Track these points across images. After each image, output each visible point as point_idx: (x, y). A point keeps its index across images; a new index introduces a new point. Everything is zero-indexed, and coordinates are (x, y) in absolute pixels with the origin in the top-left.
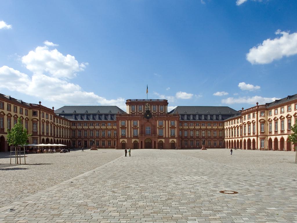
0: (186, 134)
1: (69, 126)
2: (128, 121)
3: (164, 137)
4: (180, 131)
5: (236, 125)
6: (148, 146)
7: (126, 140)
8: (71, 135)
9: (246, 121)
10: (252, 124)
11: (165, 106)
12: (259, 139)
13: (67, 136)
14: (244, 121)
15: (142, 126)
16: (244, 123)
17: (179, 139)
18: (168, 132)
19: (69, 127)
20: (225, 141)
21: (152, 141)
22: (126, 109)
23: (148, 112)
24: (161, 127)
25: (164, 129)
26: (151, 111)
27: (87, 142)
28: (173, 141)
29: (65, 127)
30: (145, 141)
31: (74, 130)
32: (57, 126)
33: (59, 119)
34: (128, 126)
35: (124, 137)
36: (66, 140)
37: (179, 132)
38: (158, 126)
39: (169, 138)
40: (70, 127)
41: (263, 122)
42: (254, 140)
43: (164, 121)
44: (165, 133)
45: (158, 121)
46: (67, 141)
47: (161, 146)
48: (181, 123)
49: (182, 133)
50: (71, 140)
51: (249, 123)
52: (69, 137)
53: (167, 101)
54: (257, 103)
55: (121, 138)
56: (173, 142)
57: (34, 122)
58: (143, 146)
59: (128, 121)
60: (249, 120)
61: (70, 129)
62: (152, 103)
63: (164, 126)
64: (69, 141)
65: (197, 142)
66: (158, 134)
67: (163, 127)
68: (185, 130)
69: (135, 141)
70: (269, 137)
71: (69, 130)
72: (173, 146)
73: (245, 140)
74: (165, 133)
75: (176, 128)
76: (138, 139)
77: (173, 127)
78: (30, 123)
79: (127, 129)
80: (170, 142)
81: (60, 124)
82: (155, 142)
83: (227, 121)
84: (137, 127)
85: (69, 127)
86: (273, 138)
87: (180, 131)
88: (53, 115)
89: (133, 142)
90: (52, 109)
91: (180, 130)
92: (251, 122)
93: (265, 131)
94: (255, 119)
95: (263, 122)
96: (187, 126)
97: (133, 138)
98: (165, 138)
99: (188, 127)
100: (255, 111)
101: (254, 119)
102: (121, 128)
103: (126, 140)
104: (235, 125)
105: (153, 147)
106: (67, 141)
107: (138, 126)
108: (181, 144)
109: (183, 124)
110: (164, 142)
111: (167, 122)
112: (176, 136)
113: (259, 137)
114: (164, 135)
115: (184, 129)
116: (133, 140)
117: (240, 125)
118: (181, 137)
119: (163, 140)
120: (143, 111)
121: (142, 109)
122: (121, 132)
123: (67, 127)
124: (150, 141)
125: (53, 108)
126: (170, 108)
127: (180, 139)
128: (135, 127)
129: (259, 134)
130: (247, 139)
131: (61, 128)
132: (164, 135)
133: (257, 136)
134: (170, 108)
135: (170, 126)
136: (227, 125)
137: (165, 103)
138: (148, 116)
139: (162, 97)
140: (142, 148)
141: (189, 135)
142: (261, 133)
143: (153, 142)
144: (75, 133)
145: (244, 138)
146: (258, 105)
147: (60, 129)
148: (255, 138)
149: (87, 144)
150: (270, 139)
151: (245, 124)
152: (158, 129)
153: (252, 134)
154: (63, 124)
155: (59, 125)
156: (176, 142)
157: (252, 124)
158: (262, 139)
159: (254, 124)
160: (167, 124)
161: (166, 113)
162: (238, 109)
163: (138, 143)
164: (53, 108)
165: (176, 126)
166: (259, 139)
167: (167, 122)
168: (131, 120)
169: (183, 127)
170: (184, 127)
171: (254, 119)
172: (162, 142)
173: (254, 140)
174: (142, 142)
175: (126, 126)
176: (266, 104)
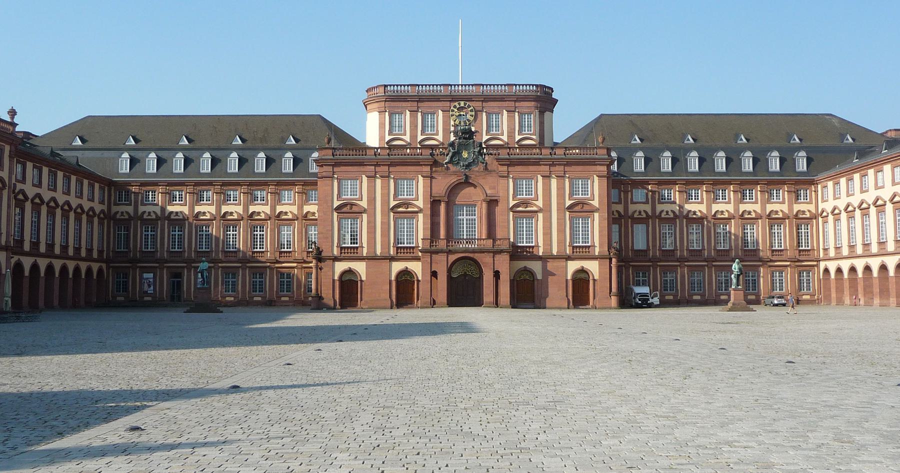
0: (640, 239)
1: (102, 202)
2: (372, 177)
5: (870, 198)
7: (360, 268)
8: (108, 243)
11: (542, 113)
13: (90, 251)
17: (611, 259)
18: (561, 231)
19: (98, 208)
20: (826, 271)
24: (524, 211)
27: (179, 275)
28: (583, 271)
29: (80, 206)
30: (449, 271)
31: (125, 223)
32: (38, 202)
33: (45, 170)
34: (372, 200)
36: (71, 265)
40: (105, 207)
46: (89, 270)
47: (526, 293)
49: (625, 236)
50: (108, 268)
52: (100, 252)
55: (336, 259)
56: (583, 276)
58: (442, 294)
59: (372, 177)
61: (107, 217)
63: (540, 203)
64: (100, 271)
67: (535, 205)
68: (639, 221)
69: (405, 272)
71: (101, 223)
75: (593, 211)
76: (417, 259)
77: (579, 209)
81: (55, 190)
82: (497, 275)
83: (835, 178)
85: (98, 208)
87: (615, 228)
88: (7, 148)
90: (9, 120)
96: (647, 202)
99: (648, 208)
102: (338, 208)
104: (879, 193)
106: (89, 270)
107: (420, 203)
109: (626, 192)
110: (539, 277)
111: (554, 182)
112: (597, 251)
115: (632, 217)
119: (536, 267)
123: (92, 209)
124: (471, 270)
125: (13, 113)
126: (565, 124)
131: (84, 217)
132: (541, 243)
134: (565, 124)
136: (834, 195)
137: (544, 100)
138: (465, 155)
141: (654, 246)
144: (127, 237)
147: (78, 219)
149: (179, 285)
154: (68, 193)
155: (47, 195)
163: (418, 281)
164: (13, 113)
165: (596, 203)
167: (554, 182)
169: (626, 208)
170: (632, 208)
172: (531, 273)
174: (434, 274)
175: (364, 204)
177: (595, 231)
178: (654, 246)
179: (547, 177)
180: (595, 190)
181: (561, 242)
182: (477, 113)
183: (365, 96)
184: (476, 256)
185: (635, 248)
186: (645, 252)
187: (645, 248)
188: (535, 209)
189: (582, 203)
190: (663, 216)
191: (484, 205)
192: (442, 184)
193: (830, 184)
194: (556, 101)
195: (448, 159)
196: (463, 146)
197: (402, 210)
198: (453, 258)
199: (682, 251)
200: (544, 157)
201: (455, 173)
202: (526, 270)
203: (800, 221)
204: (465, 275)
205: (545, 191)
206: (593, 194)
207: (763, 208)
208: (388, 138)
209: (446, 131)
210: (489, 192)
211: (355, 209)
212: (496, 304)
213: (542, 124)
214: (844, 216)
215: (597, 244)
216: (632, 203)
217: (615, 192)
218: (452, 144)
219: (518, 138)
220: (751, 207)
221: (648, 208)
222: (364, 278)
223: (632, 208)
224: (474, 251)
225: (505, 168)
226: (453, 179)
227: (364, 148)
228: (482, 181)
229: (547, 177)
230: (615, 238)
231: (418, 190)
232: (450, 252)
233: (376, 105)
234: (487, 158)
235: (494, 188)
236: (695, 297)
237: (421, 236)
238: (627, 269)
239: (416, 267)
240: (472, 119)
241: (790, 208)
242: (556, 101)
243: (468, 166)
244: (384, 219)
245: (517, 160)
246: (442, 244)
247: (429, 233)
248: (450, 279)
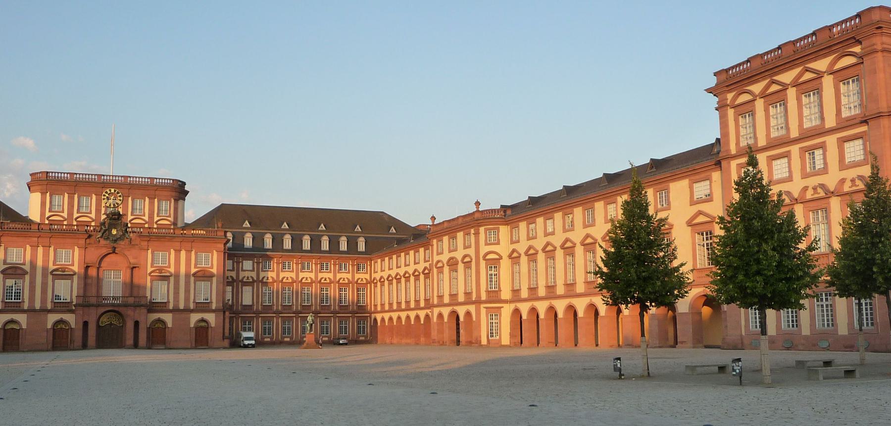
0: (247, 297)
3: (171, 307)
4: (229, 289)
7: (22, 318)
9: (445, 257)
10: (461, 267)
11: (176, 200)
12: (483, 312)
14: (436, 258)
16: (438, 262)
17: (224, 312)
18: (187, 291)
20: (375, 319)
21: (124, 322)
23: (115, 218)
25: (172, 279)
26: (126, 215)
37: (224, 292)
38: (150, 270)
39: (187, 310)
42: (468, 314)
43: (172, 252)
44: (176, 293)
45: (150, 251)
47: (158, 338)
49: (236, 294)
51: (453, 264)
53: (184, 184)
54: (478, 204)
56: (203, 324)
60: (452, 255)
62: (129, 187)
65: (284, 323)
66: (148, 295)
69: (61, 321)
70: (512, 306)
72: (201, 338)
73: (440, 316)
74: (176, 293)
76: (72, 311)
79: (27, 277)
80: (192, 325)
82: (137, 324)
84: (72, 270)
86: (525, 308)
87: (229, 289)
89: (49, 326)
91: (229, 284)
92: (460, 259)
93: (500, 288)
94: (471, 252)
96: (253, 270)
97: (50, 311)
98: (176, 310)
99: (254, 274)
100: (472, 227)
101: (468, 251)
103: (22, 318)
105: (130, 341)
108: (231, 329)
109: (238, 263)
110: (170, 325)
111: (183, 254)
113: (482, 306)
114: (171, 300)
115: (242, 281)
116: (52, 318)
117: (425, 268)
118: (232, 306)
119: (168, 318)
120: (93, 215)
126: (194, 209)
127: (227, 313)
129: (484, 297)
130: (446, 311)
132: (171, 300)
135: (193, 270)
136: (384, 268)
137: (179, 191)
138: (114, 232)
139: (165, 172)
140: (85, 346)
141: (257, 302)
142: (488, 292)
143: (130, 326)
145: (436, 311)
146: (480, 209)
148: (472, 308)
150: (517, 312)
151: (440, 265)
152: (149, 278)
153: (461, 298)
156: (213, 325)
157: (461, 267)
159: (467, 265)
161: (180, 225)
162: (413, 220)
165: (214, 270)
166: (483, 312)
167: (183, 254)
168: (47, 247)
170: (242, 275)
171: (468, 251)
173: (468, 314)
174: (86, 324)
175: (27, 268)
176: (502, 206)
178: (257, 302)
179: (178, 251)
181: (187, 299)
182: (125, 198)
183: (29, 179)
184: (121, 309)
185: (244, 303)
186: (251, 306)
187: (251, 303)
188: (168, 274)
189: (203, 271)
190: (265, 280)
191: (129, 271)
192: (94, 254)
193: (379, 260)
194: (188, 192)
195: (100, 235)
196: (112, 226)
198: (102, 310)
199: (277, 306)
200: (179, 235)
201: (105, 246)
202: (160, 320)
203: (360, 287)
204: (111, 324)
205: (178, 261)
206: (212, 264)
207: (335, 276)
208: (48, 214)
209: (98, 211)
210: (132, 261)
211: (19, 272)
212: (136, 346)
213: (176, 209)
214: (386, 283)
215: (214, 301)
216: (242, 270)
217: (229, 263)
218: (103, 224)
219: (156, 219)
220: (327, 275)
221: (254, 274)
222: (24, 326)
223: (242, 275)
224: (119, 305)
225: (146, 243)
226: (104, 251)
227: (26, 221)
228: (127, 253)
229: (178, 251)
230: (229, 296)
232: (98, 306)
233: (40, 187)
234: (131, 235)
235: (136, 258)
236: (286, 339)
237: (75, 293)
238: (237, 319)
239: (70, 318)
240: (120, 202)
241: (353, 276)
242: (188, 192)
243: (115, 241)
245: (155, 237)
246: (93, 301)
247: (81, 292)
248: (98, 326)
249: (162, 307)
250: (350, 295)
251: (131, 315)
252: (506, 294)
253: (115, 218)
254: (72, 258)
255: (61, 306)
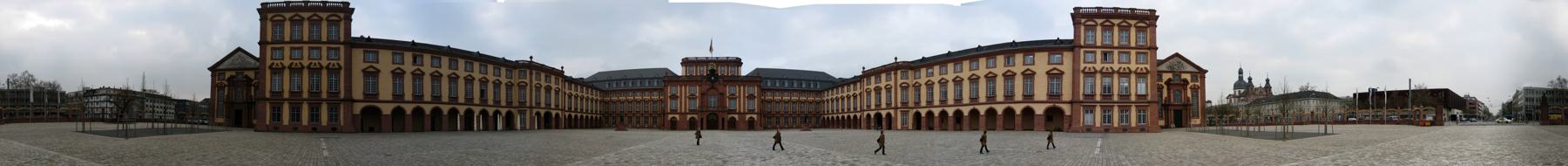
0: (768, 108)
6: (713, 125)
15: (702, 94)
22: (679, 70)
23: (713, 72)
24: (733, 97)
35: (674, 111)
41: (905, 88)
47: (732, 125)
48: (763, 90)
57: (522, 87)
62: (719, 62)
72: (751, 126)
78: (515, 90)
95: (905, 88)
121: (704, 71)
122: (670, 104)
126: (745, 71)
128: (692, 97)
133: (896, 108)
137: (738, 62)
158: (905, 113)
160: (741, 91)
177: (755, 104)
180: (755, 90)
197: (692, 97)
231: (697, 90)
244: (685, 101)
249: (734, 112)
250: (812, 108)
251: (721, 116)
252: (911, 104)
253: (713, 72)
254: (697, 90)
255: (692, 112)
